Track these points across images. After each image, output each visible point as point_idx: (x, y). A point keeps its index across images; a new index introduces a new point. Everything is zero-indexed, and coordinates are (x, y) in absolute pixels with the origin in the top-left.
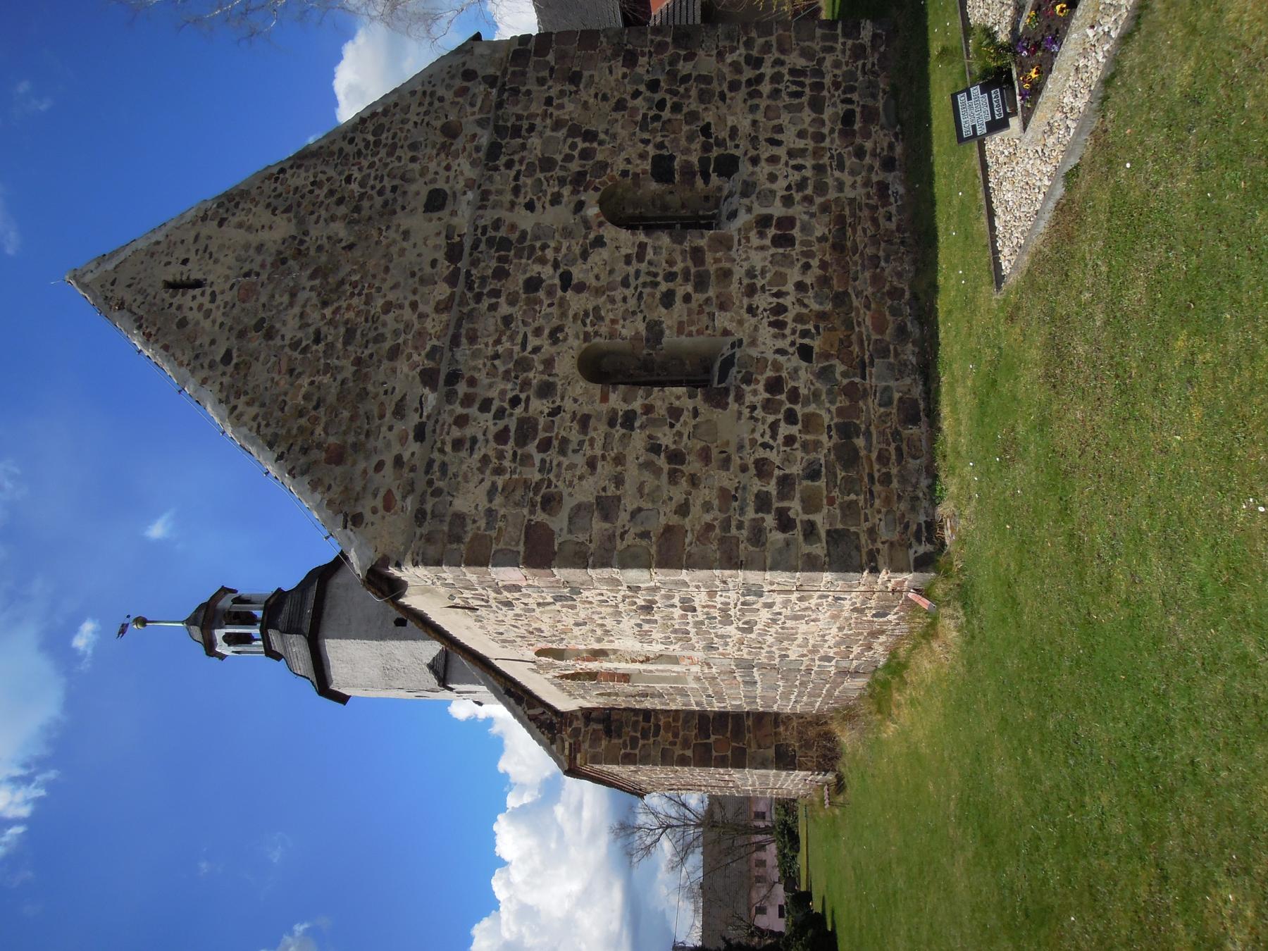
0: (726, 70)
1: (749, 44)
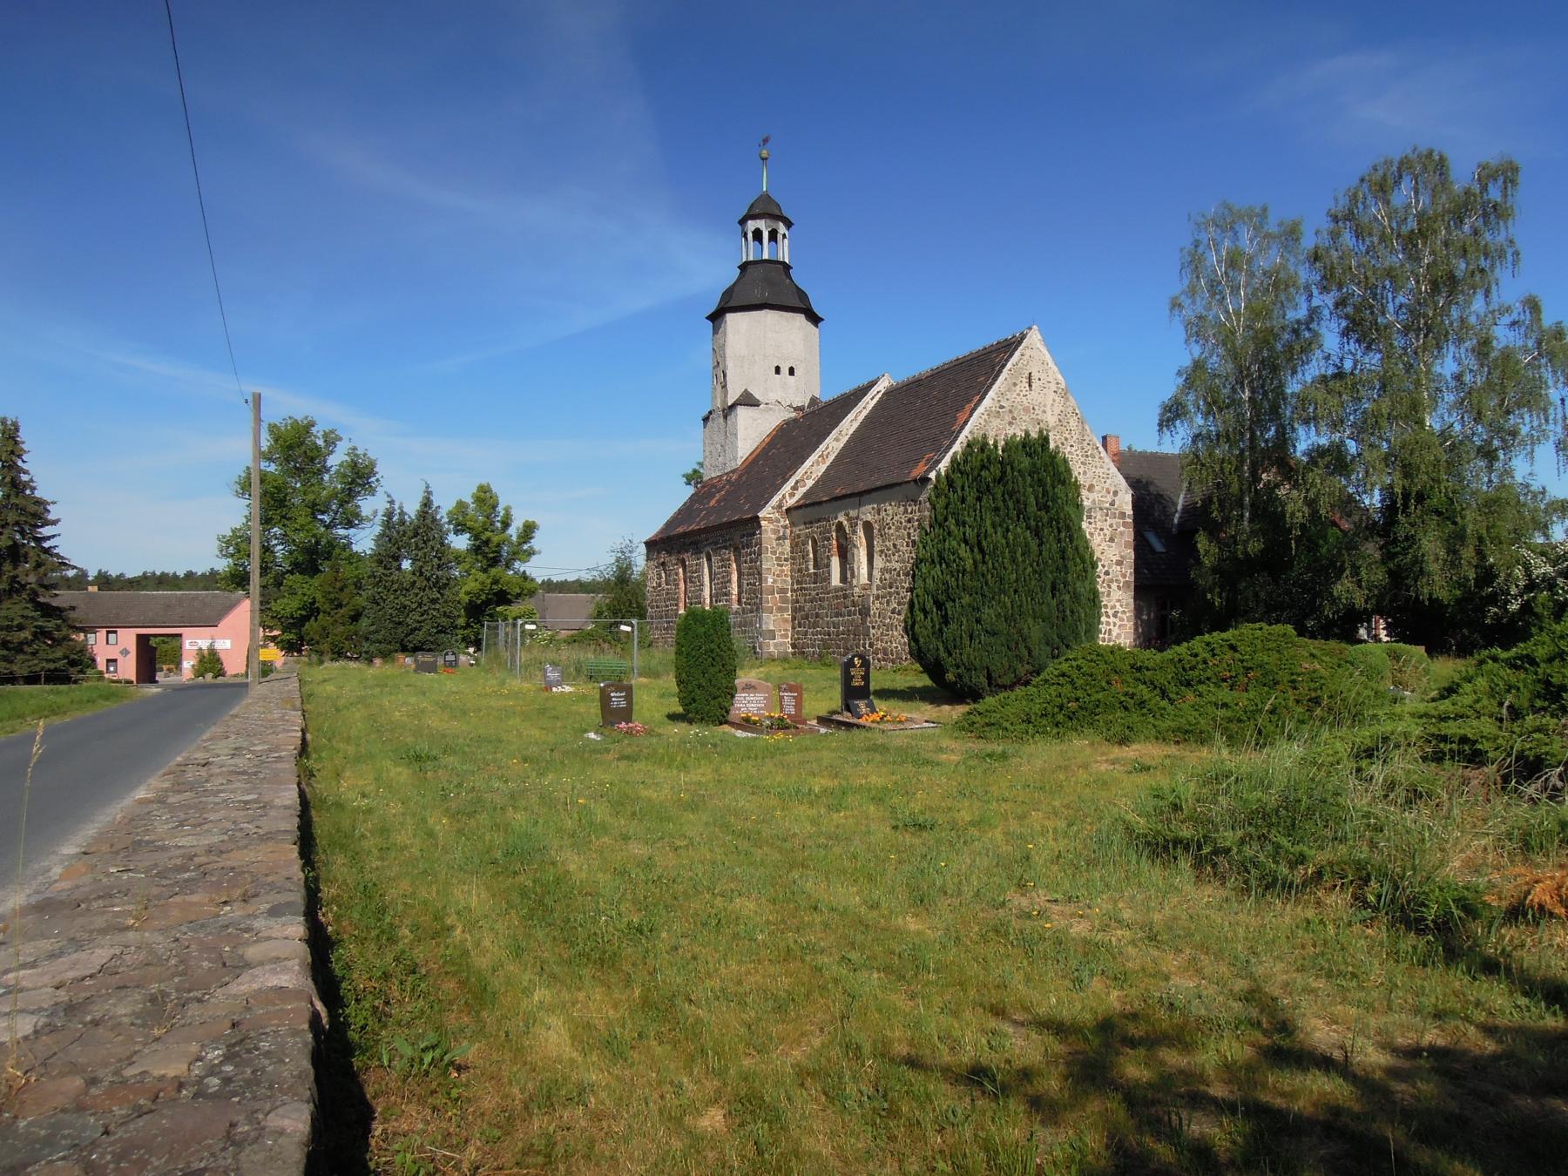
0: (1112, 603)
1: (1124, 612)
